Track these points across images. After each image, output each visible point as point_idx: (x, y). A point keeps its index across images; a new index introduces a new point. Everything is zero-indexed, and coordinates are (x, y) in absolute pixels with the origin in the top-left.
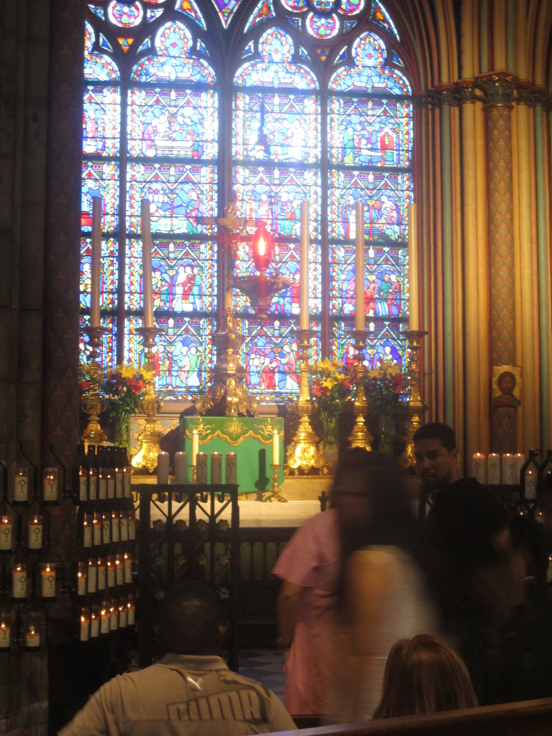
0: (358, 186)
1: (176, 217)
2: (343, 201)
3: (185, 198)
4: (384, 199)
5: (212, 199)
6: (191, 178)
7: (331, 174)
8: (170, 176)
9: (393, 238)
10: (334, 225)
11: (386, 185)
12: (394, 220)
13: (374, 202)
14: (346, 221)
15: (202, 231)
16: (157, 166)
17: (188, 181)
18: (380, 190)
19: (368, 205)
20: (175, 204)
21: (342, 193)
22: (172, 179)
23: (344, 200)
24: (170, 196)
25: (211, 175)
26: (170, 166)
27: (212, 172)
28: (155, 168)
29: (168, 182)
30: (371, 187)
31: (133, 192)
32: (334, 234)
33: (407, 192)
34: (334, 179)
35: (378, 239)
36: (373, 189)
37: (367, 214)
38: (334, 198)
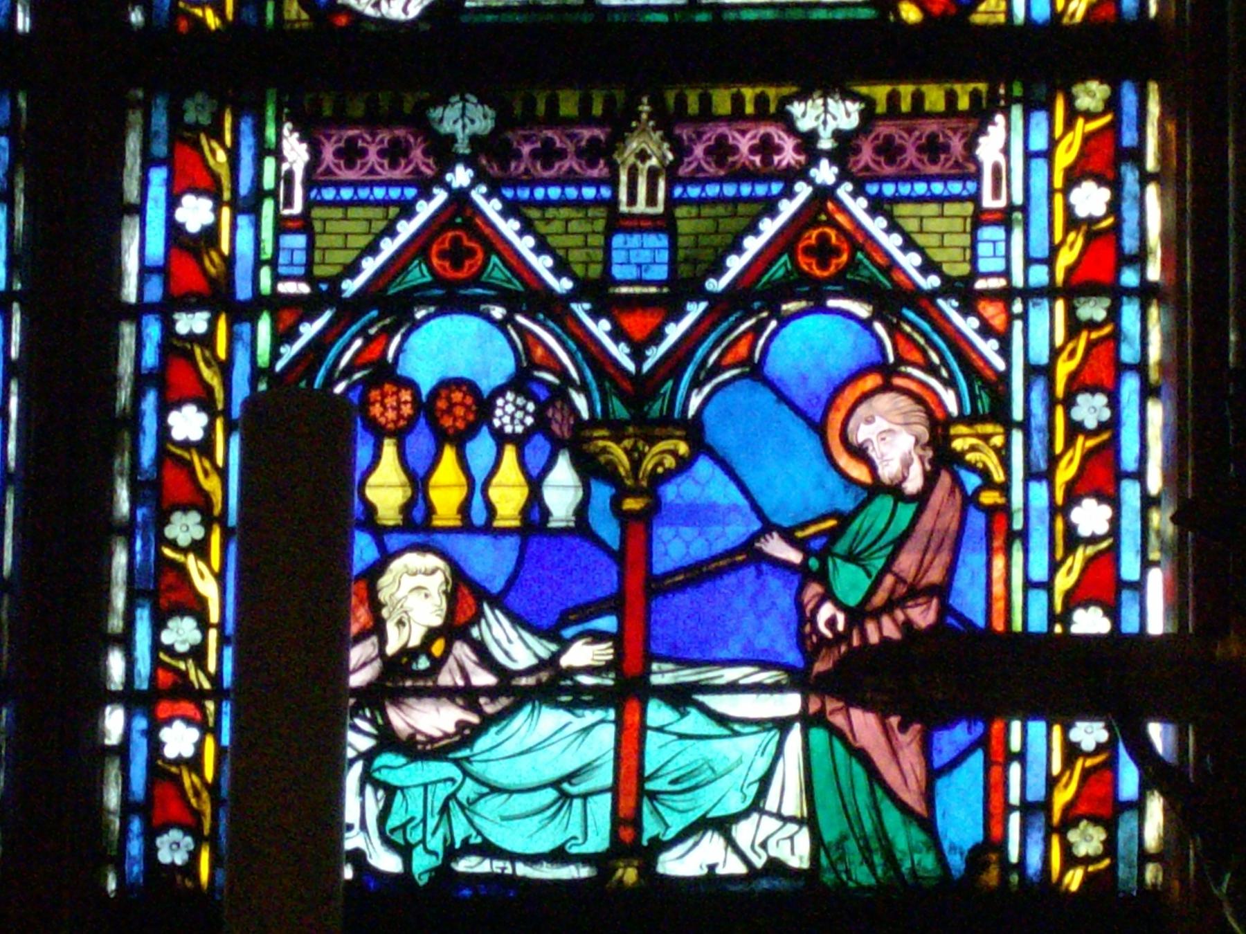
1: (680, 697)
3: (796, 482)
5: (1103, 475)
6: (859, 241)
8: (618, 223)
15: (992, 844)
16: (463, 120)
17: (821, 265)
20: (674, 547)
22: (641, 260)
24: (618, 452)
25: (1091, 199)
26: (620, 124)
27: (1106, 159)
28: (443, 152)
29: (598, 291)
31: (188, 423)
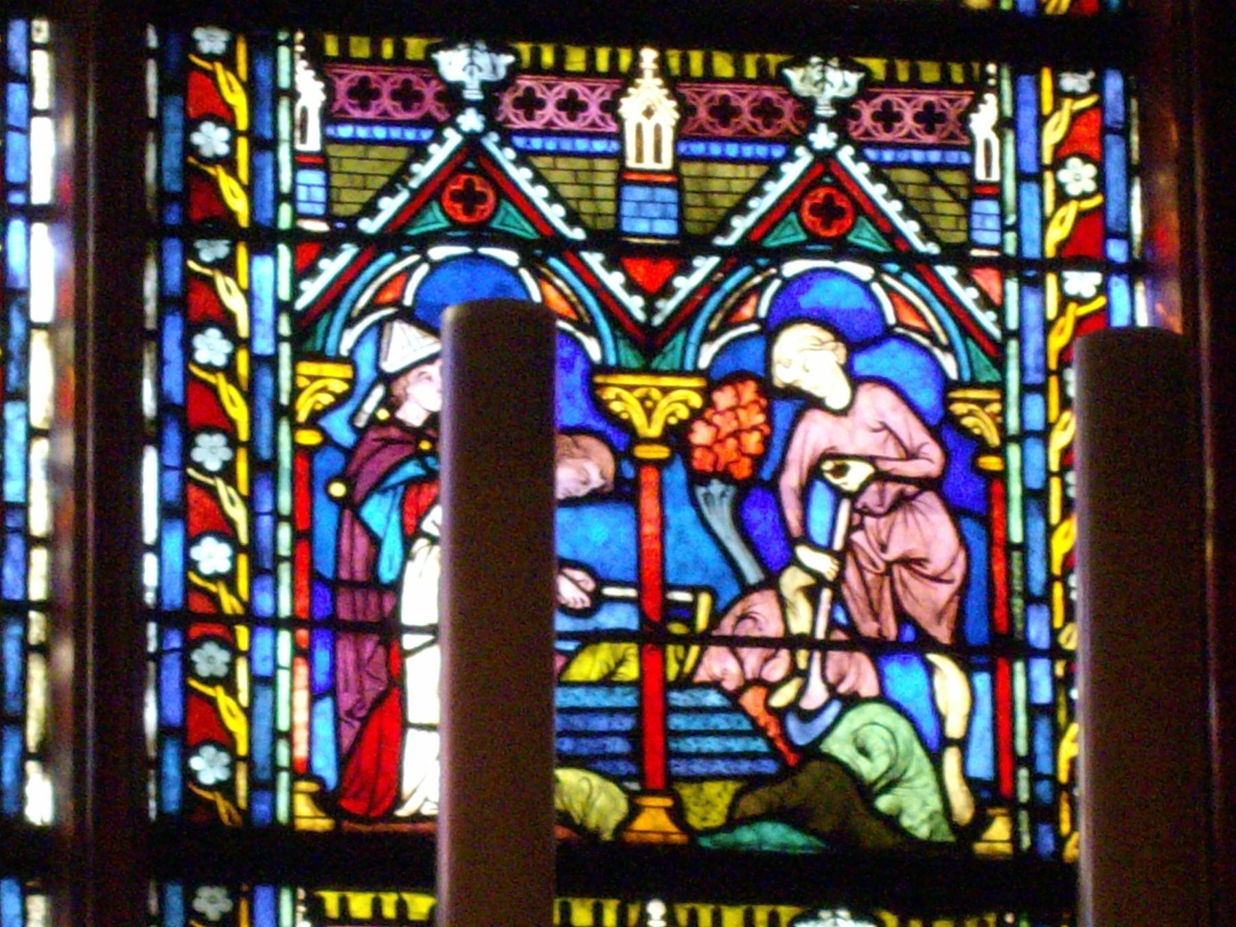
0: (510, 220)
2: (321, 383)
4: (806, 358)
7: (184, 79)
9: (917, 808)
10: (210, 658)
11: (828, 210)
12: (930, 601)
13: (681, 398)
14: (350, 615)
18: (751, 251)
19: (620, 437)
21: (311, 290)
23: (334, 377)
30: (650, 219)
32: (208, 767)
33: (1082, 282)
34: (212, 139)
35: (733, 821)
36: (681, 250)
37: (592, 535)
38: (211, 347)
